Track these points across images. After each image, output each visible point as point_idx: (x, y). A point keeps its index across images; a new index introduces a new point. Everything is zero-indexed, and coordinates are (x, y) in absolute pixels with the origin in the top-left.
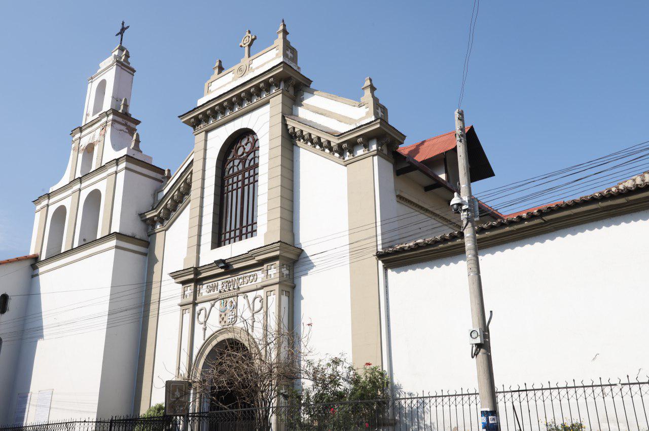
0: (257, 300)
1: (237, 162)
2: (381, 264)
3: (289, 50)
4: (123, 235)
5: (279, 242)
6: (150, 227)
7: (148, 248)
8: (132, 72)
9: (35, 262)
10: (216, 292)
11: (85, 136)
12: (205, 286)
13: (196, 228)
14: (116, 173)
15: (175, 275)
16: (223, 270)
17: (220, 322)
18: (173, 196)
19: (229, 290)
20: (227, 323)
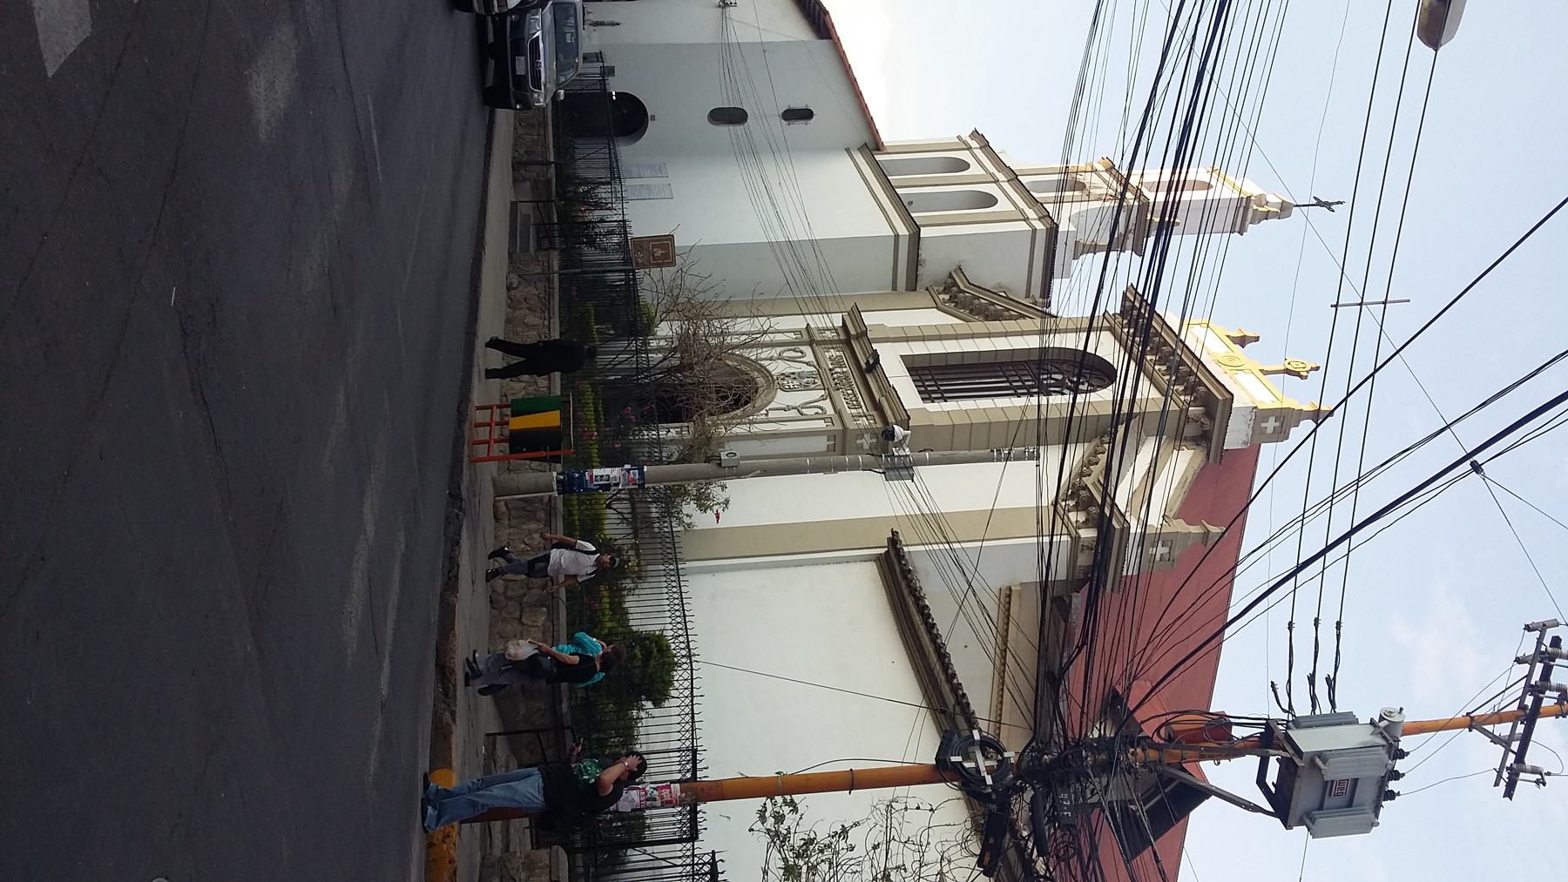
0: (820, 411)
1: (1059, 377)
2: (883, 551)
3: (1278, 424)
4: (919, 243)
5: (909, 416)
6: (942, 289)
7: (906, 290)
8: (1237, 229)
9: (872, 145)
10: (831, 367)
11: (1100, 176)
12: (841, 353)
13: (934, 332)
14: (1026, 219)
15: (855, 314)
16: (864, 366)
17: (783, 374)
18: (993, 304)
19: (834, 379)
20: (780, 382)
